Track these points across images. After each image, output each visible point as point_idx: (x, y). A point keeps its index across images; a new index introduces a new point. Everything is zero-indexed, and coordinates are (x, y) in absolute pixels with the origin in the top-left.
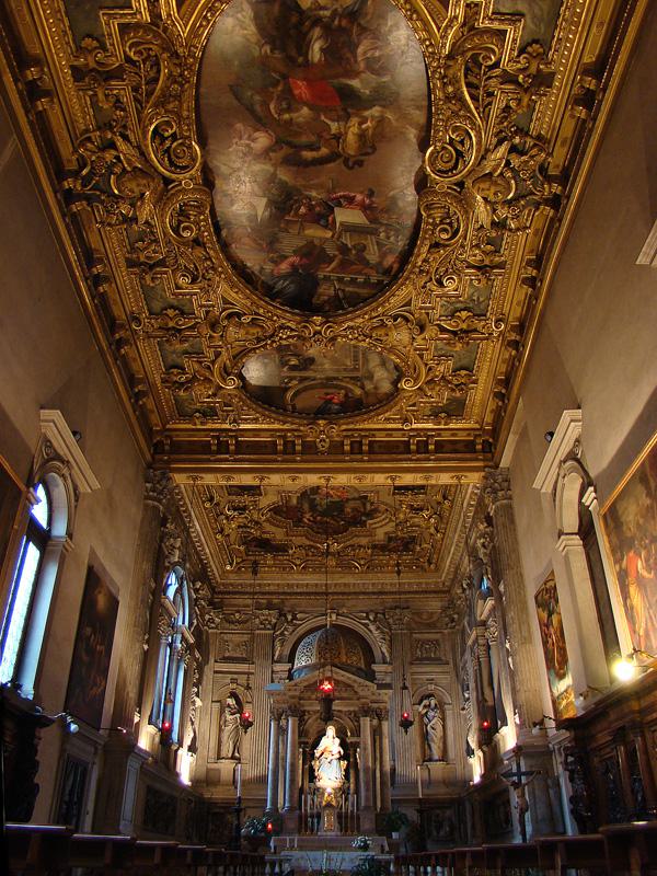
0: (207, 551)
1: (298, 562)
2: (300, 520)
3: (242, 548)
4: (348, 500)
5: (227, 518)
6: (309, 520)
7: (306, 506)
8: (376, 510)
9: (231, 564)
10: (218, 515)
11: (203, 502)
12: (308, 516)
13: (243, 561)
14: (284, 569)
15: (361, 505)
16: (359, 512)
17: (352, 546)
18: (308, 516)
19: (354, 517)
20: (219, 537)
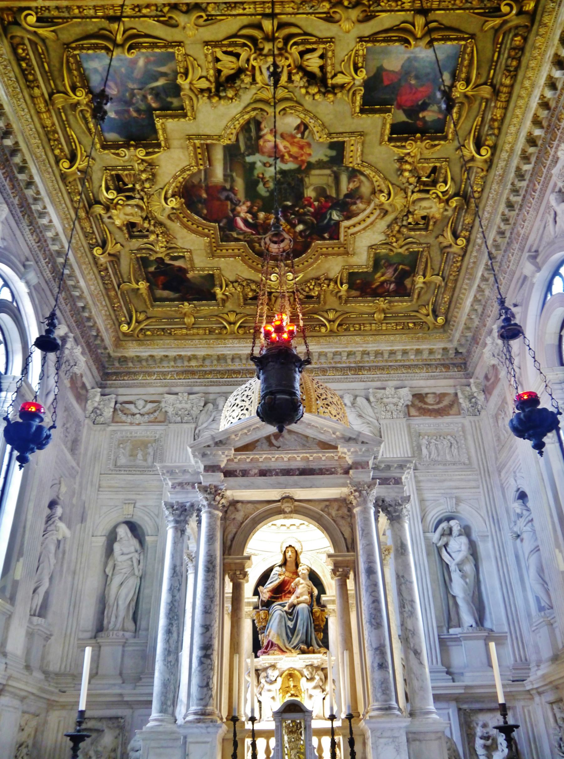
0: (82, 283)
1: (232, 318)
2: (231, 225)
3: (143, 286)
4: (311, 166)
5: (107, 209)
6: (245, 221)
7: (240, 185)
8: (354, 195)
9: (129, 324)
10: (90, 206)
11: (57, 162)
12: (243, 209)
13: (148, 318)
14: (211, 332)
15: (331, 180)
16: (328, 197)
17: (318, 279)
18: (243, 209)
19: (320, 214)
20: (97, 251)
